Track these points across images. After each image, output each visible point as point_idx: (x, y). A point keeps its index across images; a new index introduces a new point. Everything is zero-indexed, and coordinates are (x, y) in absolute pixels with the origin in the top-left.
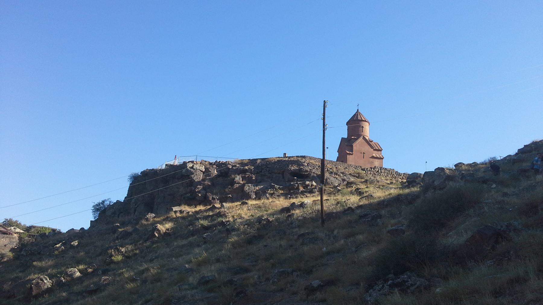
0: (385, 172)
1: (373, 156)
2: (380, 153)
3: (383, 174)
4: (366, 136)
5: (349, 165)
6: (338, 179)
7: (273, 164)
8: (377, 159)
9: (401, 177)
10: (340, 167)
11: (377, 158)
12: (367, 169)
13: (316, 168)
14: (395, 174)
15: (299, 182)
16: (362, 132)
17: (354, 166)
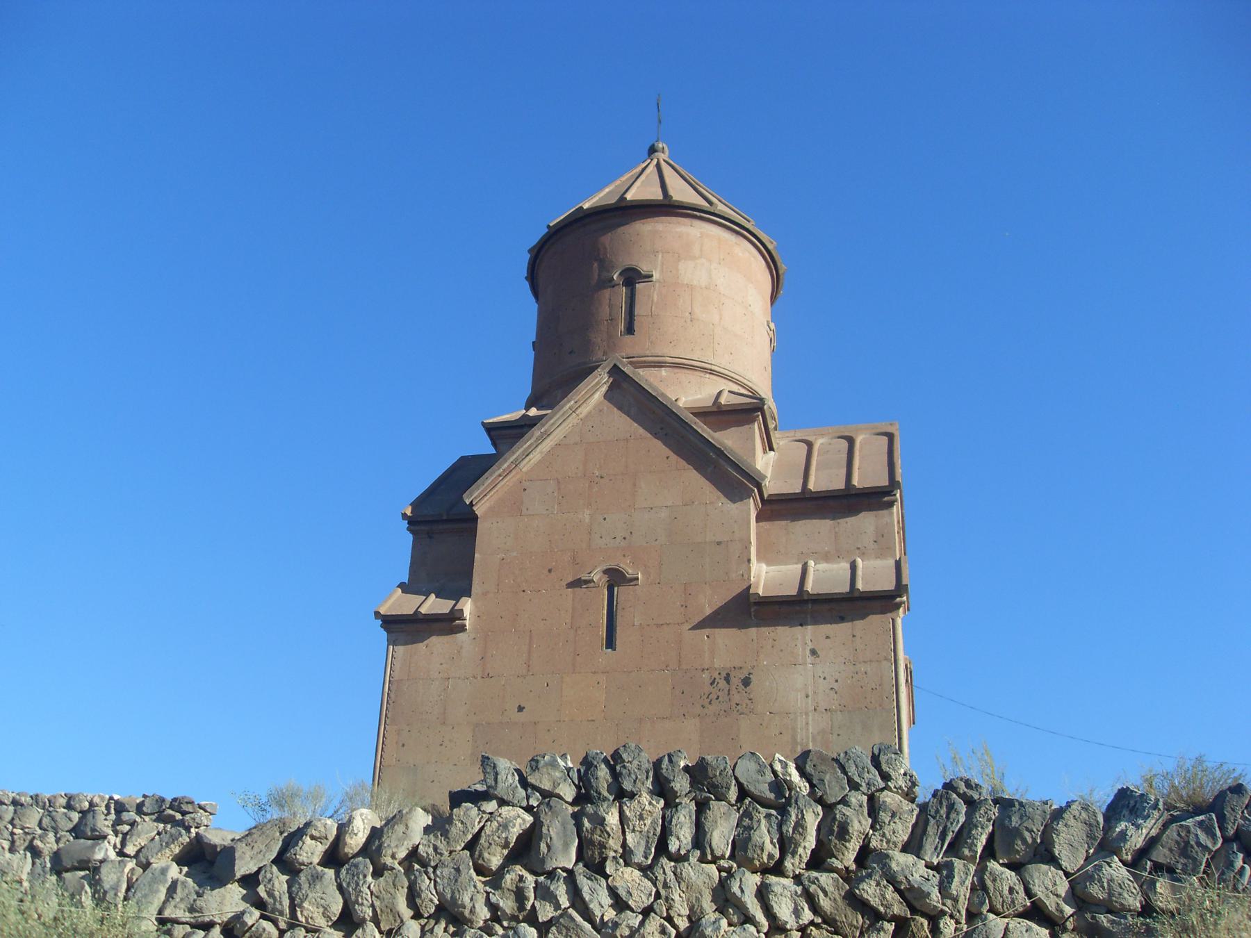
3: (628, 878)
14: (913, 846)
16: (630, 330)
17: (33, 818)
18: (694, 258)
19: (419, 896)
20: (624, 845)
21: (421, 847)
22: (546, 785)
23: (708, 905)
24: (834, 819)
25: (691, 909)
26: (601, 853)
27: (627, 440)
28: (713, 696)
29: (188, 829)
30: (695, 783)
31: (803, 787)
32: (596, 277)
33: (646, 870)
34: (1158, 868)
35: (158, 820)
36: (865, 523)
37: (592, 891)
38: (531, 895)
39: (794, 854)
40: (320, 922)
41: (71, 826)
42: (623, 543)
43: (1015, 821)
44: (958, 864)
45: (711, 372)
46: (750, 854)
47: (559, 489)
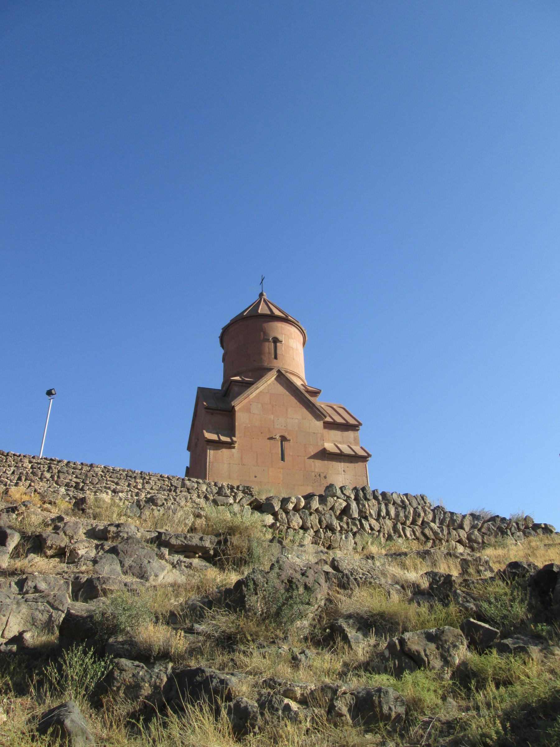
0: (383, 513)
1: (324, 450)
2: (352, 440)
4: (291, 373)
5: (173, 488)
6: (31, 583)
8: (344, 462)
9: (463, 534)
10: (106, 497)
11: (340, 457)
12: (285, 501)
14: (434, 521)
16: (276, 358)
17: (204, 488)
18: (292, 339)
19: (322, 522)
20: (370, 512)
21: (320, 508)
22: (348, 494)
23: (392, 532)
24: (417, 512)
25: (388, 532)
26: (365, 514)
28: (316, 480)
29: (253, 496)
30: (383, 498)
31: (407, 502)
33: (377, 520)
34: (483, 533)
35: (243, 493)
36: (350, 434)
37: (366, 524)
38: (350, 523)
39: (409, 520)
40: (297, 528)
41: (216, 491)
43: (455, 517)
44: (444, 527)
45: (299, 378)
46: (399, 519)
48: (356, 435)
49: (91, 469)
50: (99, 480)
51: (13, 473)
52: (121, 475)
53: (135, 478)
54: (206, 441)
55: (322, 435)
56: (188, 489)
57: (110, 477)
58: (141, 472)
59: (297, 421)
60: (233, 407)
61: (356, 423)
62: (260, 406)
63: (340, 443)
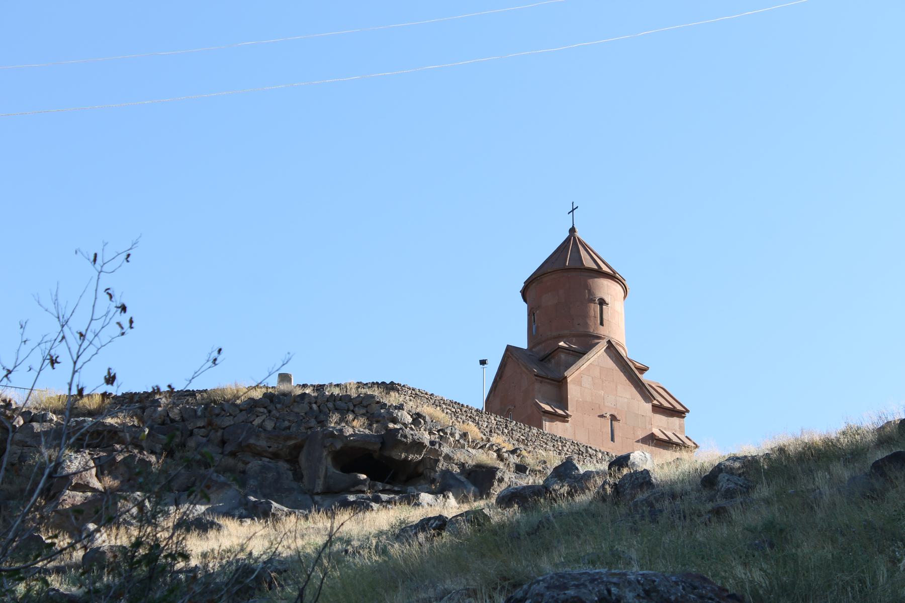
2: (677, 427)
7: (241, 411)
11: (666, 444)
13: (452, 439)
15: (384, 497)
16: (602, 324)
17: (600, 455)
27: (613, 370)
32: (587, 296)
36: (676, 420)
42: (615, 407)
45: (624, 349)
47: (593, 381)
48: (682, 422)
49: (530, 430)
50: (536, 440)
51: (487, 427)
52: (548, 437)
53: (557, 441)
54: (543, 412)
55: (651, 420)
56: (590, 455)
57: (542, 438)
58: (560, 437)
59: (626, 400)
60: (566, 378)
61: (684, 410)
62: (590, 379)
63: (665, 429)
